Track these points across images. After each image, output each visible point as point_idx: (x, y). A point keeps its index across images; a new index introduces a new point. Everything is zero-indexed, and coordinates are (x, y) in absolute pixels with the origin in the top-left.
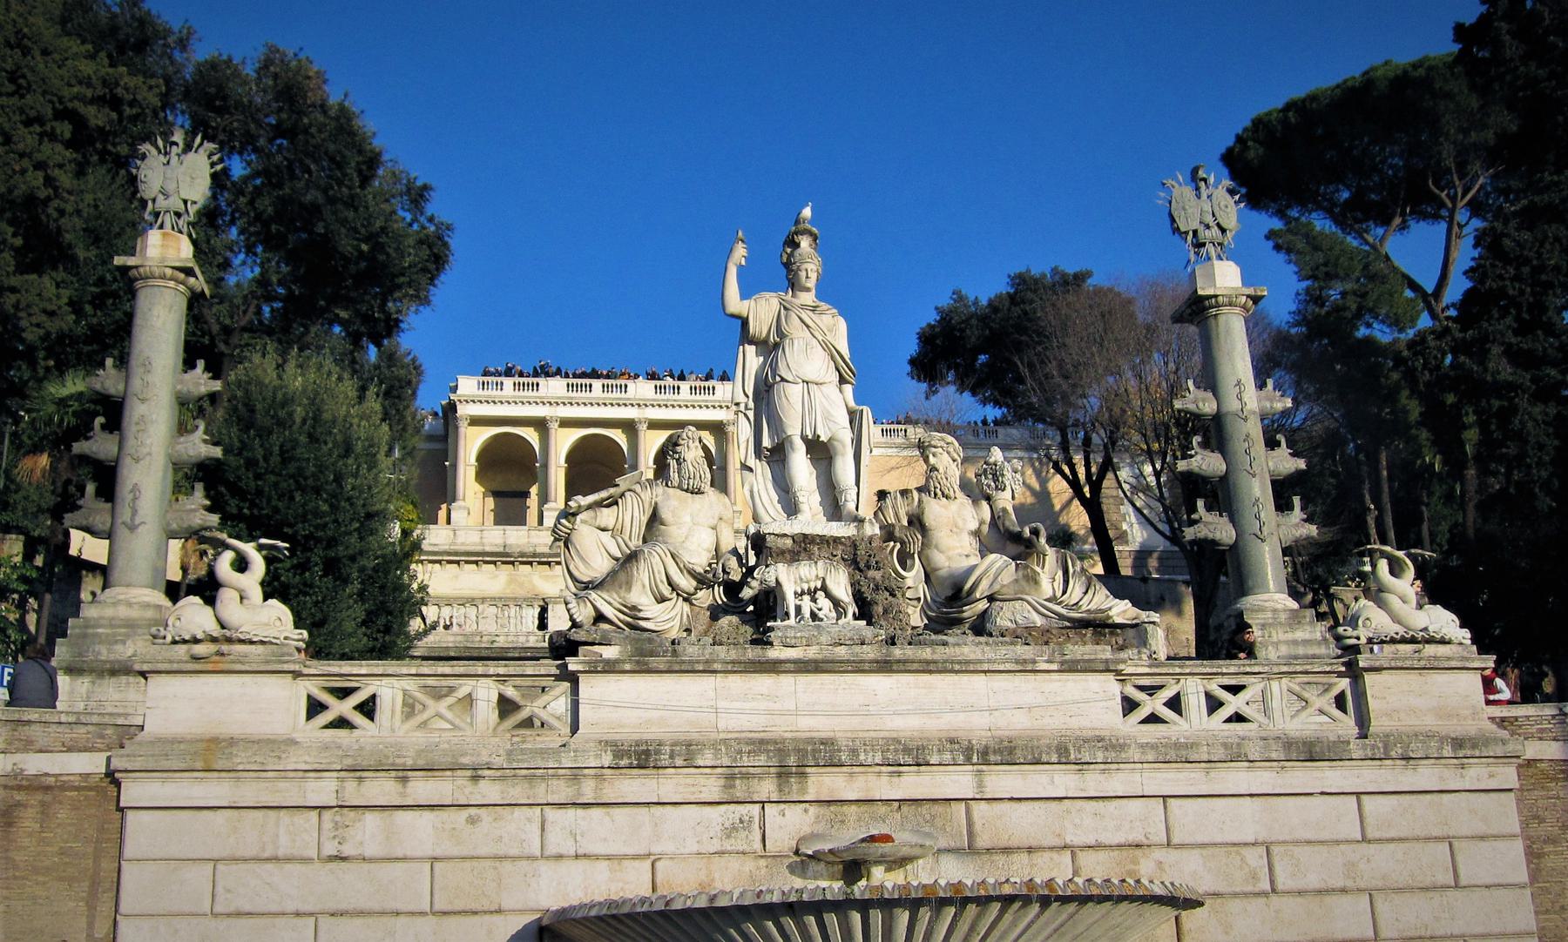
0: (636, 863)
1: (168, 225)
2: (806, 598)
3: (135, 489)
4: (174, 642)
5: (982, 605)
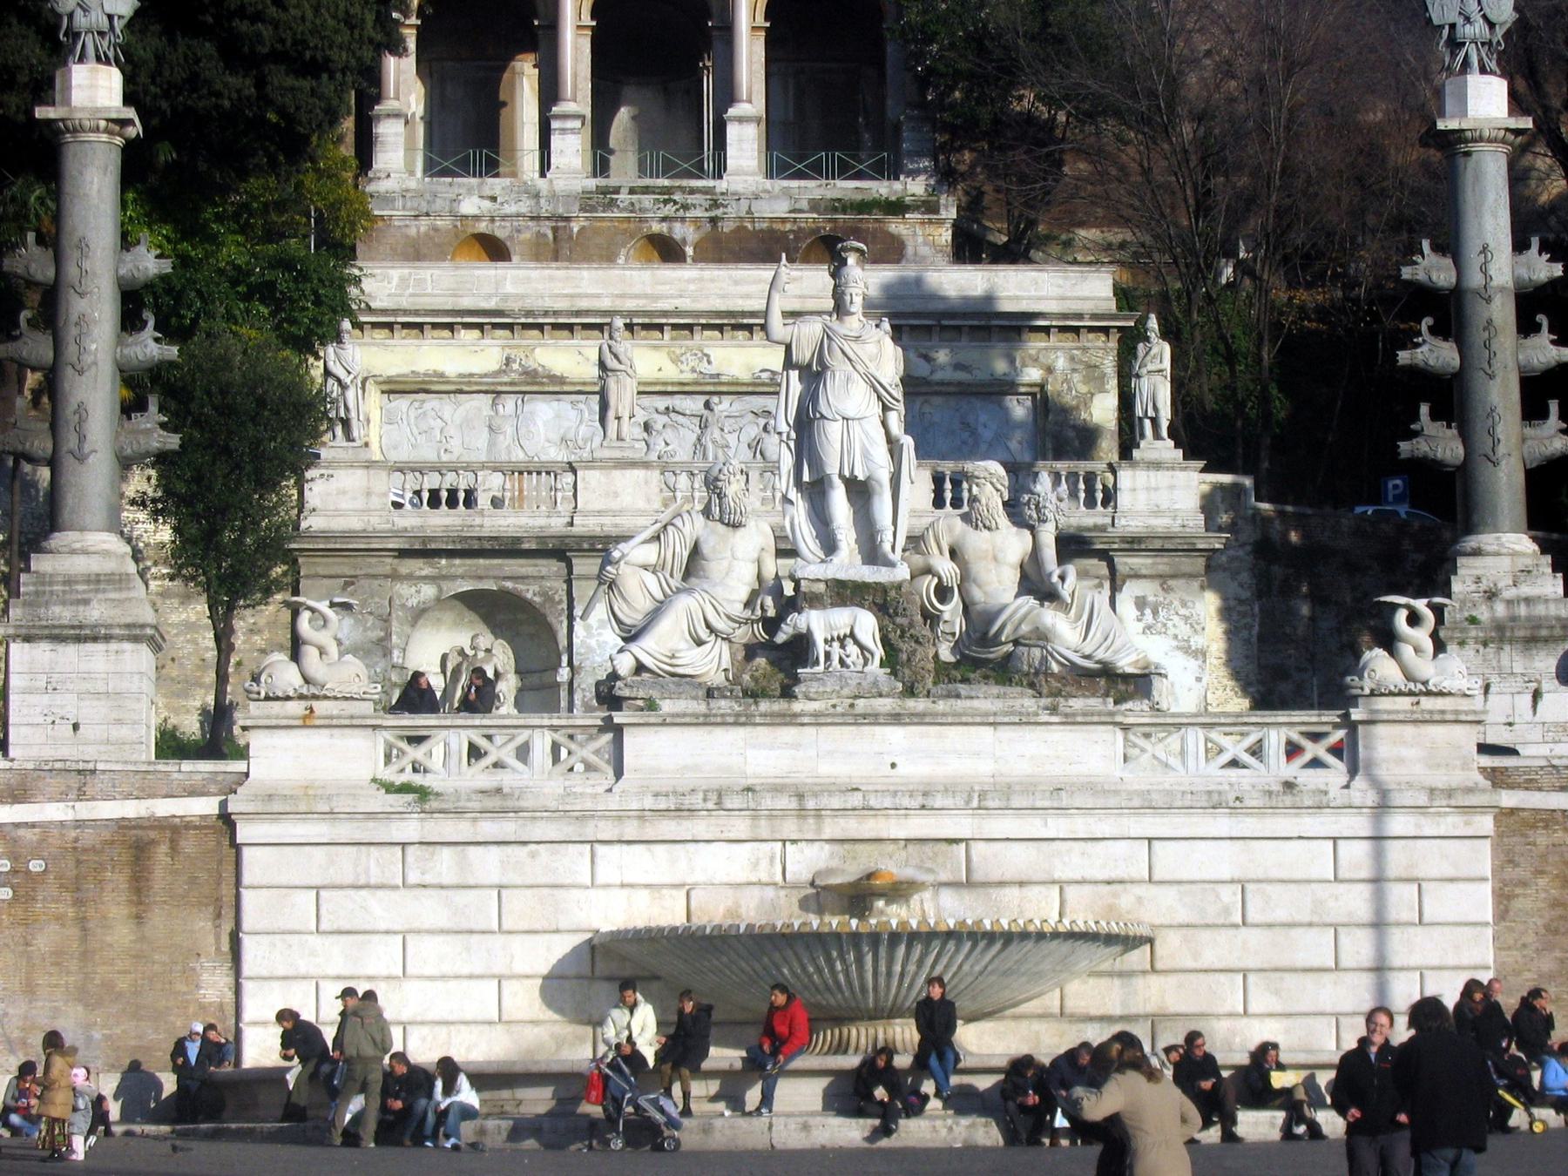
0: (674, 892)
1: (91, 51)
2: (836, 644)
3: (81, 410)
4: (267, 698)
5: (1010, 647)
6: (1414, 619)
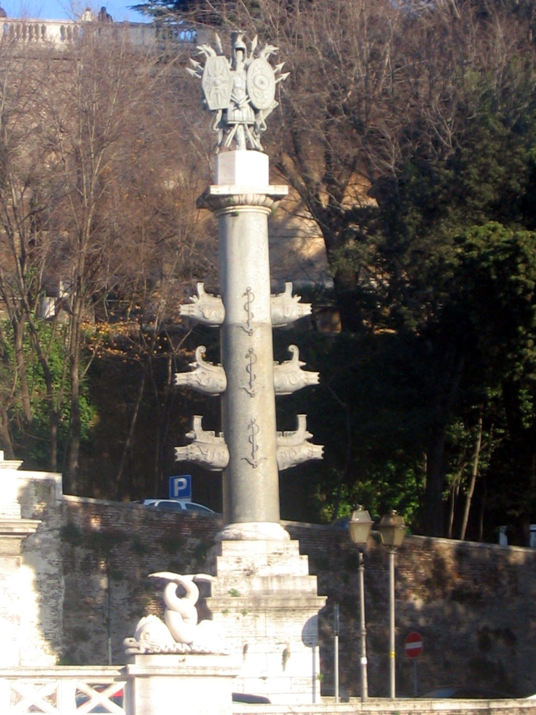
6: (182, 593)
